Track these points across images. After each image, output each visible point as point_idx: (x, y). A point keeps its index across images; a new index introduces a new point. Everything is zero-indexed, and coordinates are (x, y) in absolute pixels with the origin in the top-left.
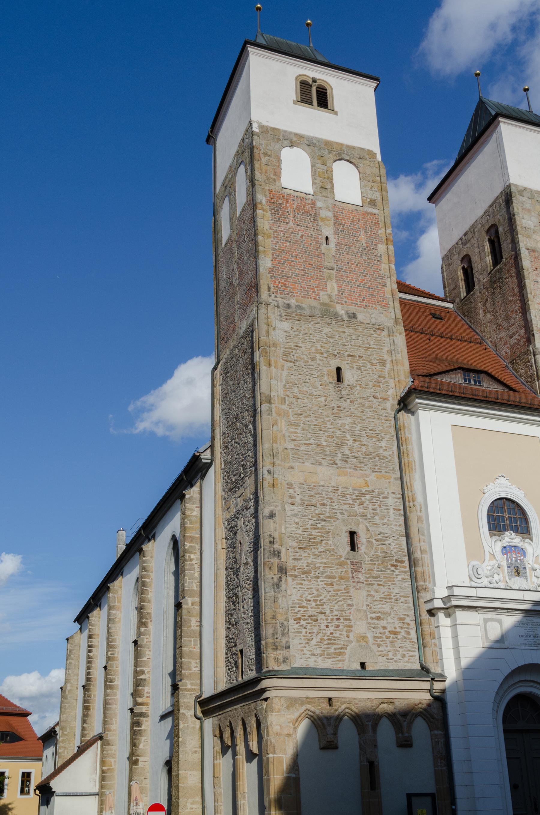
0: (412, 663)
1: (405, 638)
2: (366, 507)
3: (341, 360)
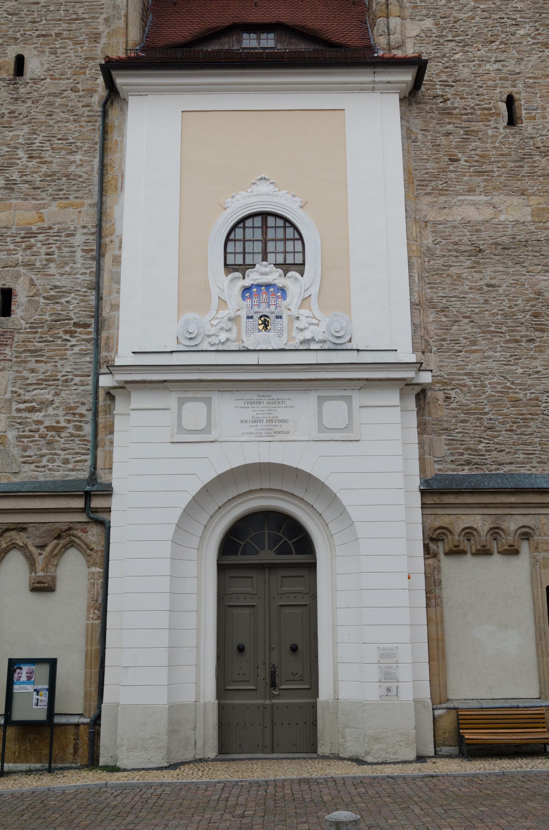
0: (79, 470)
1: (72, 435)
2: (36, 252)
3: (25, 44)
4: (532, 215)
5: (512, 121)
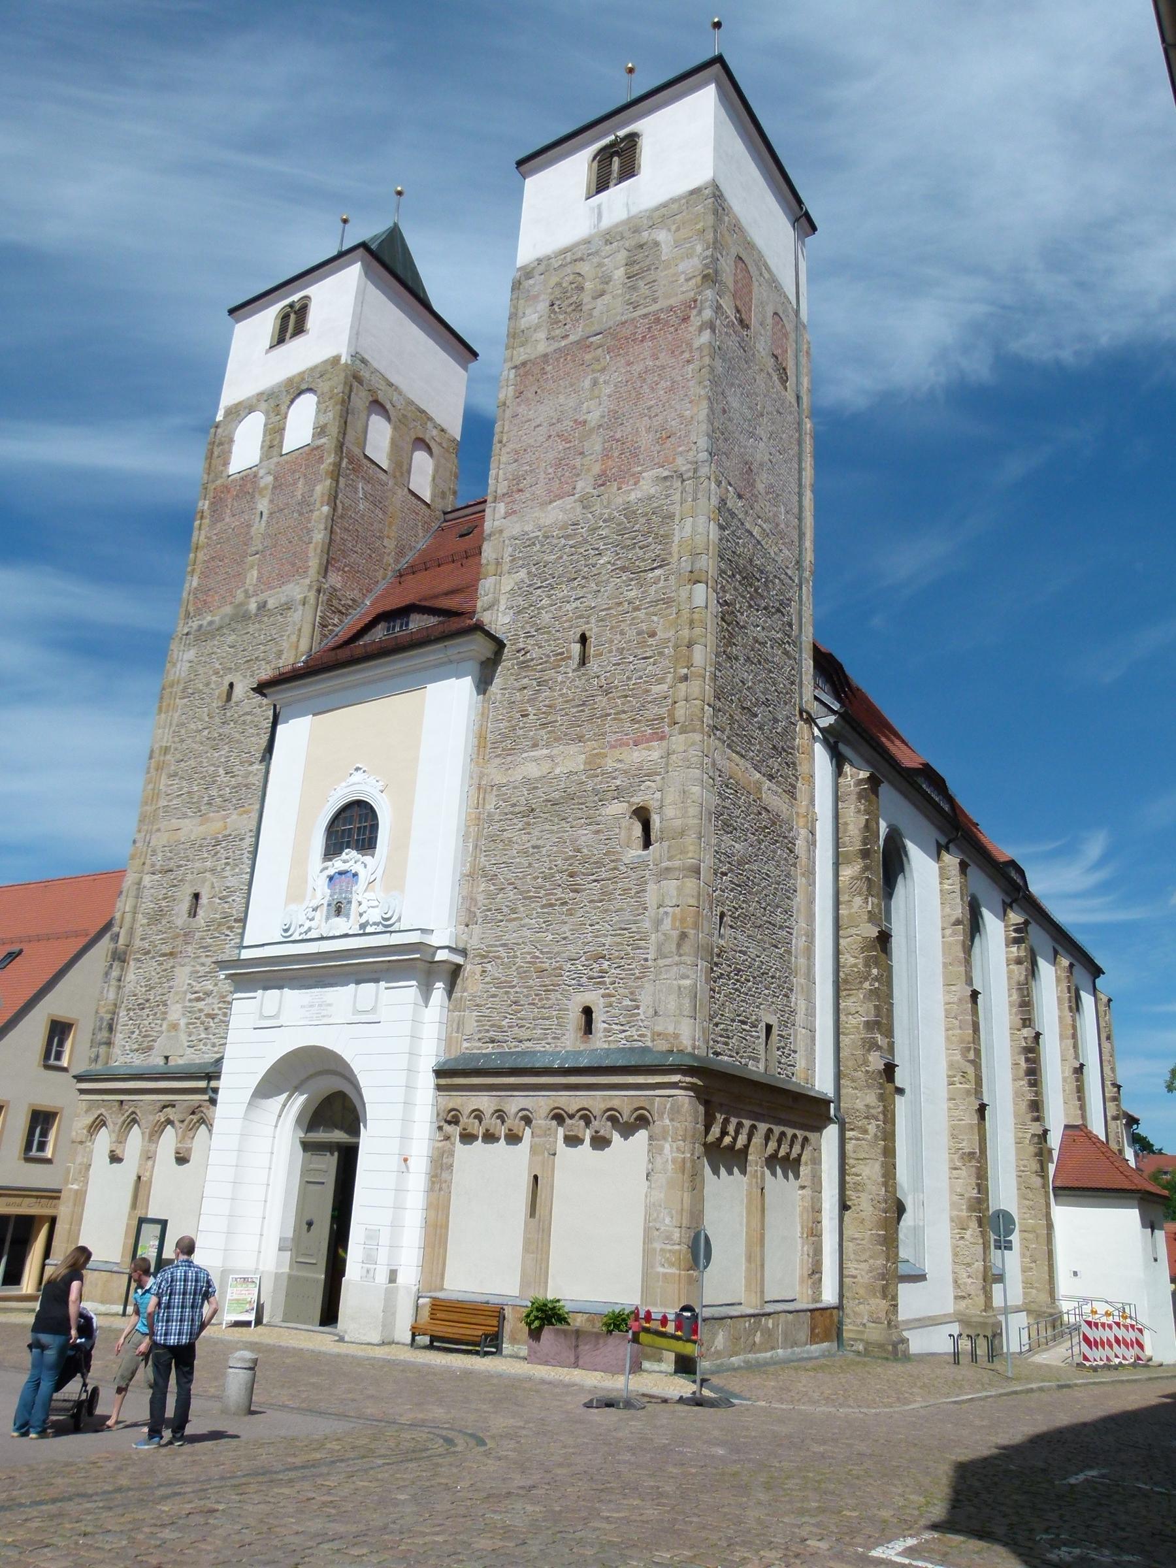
4: (585, 763)
5: (583, 661)
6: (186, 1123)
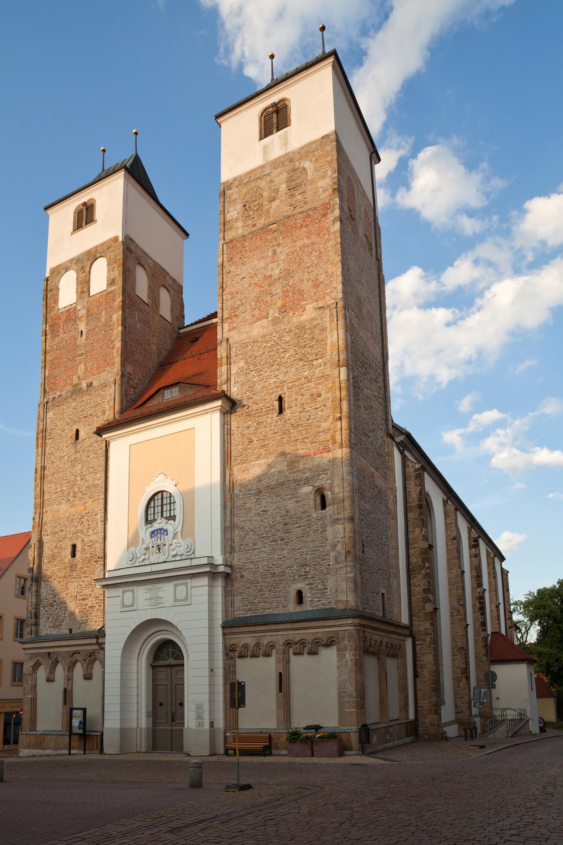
4: (287, 466)
5: (281, 411)
6: (87, 661)
